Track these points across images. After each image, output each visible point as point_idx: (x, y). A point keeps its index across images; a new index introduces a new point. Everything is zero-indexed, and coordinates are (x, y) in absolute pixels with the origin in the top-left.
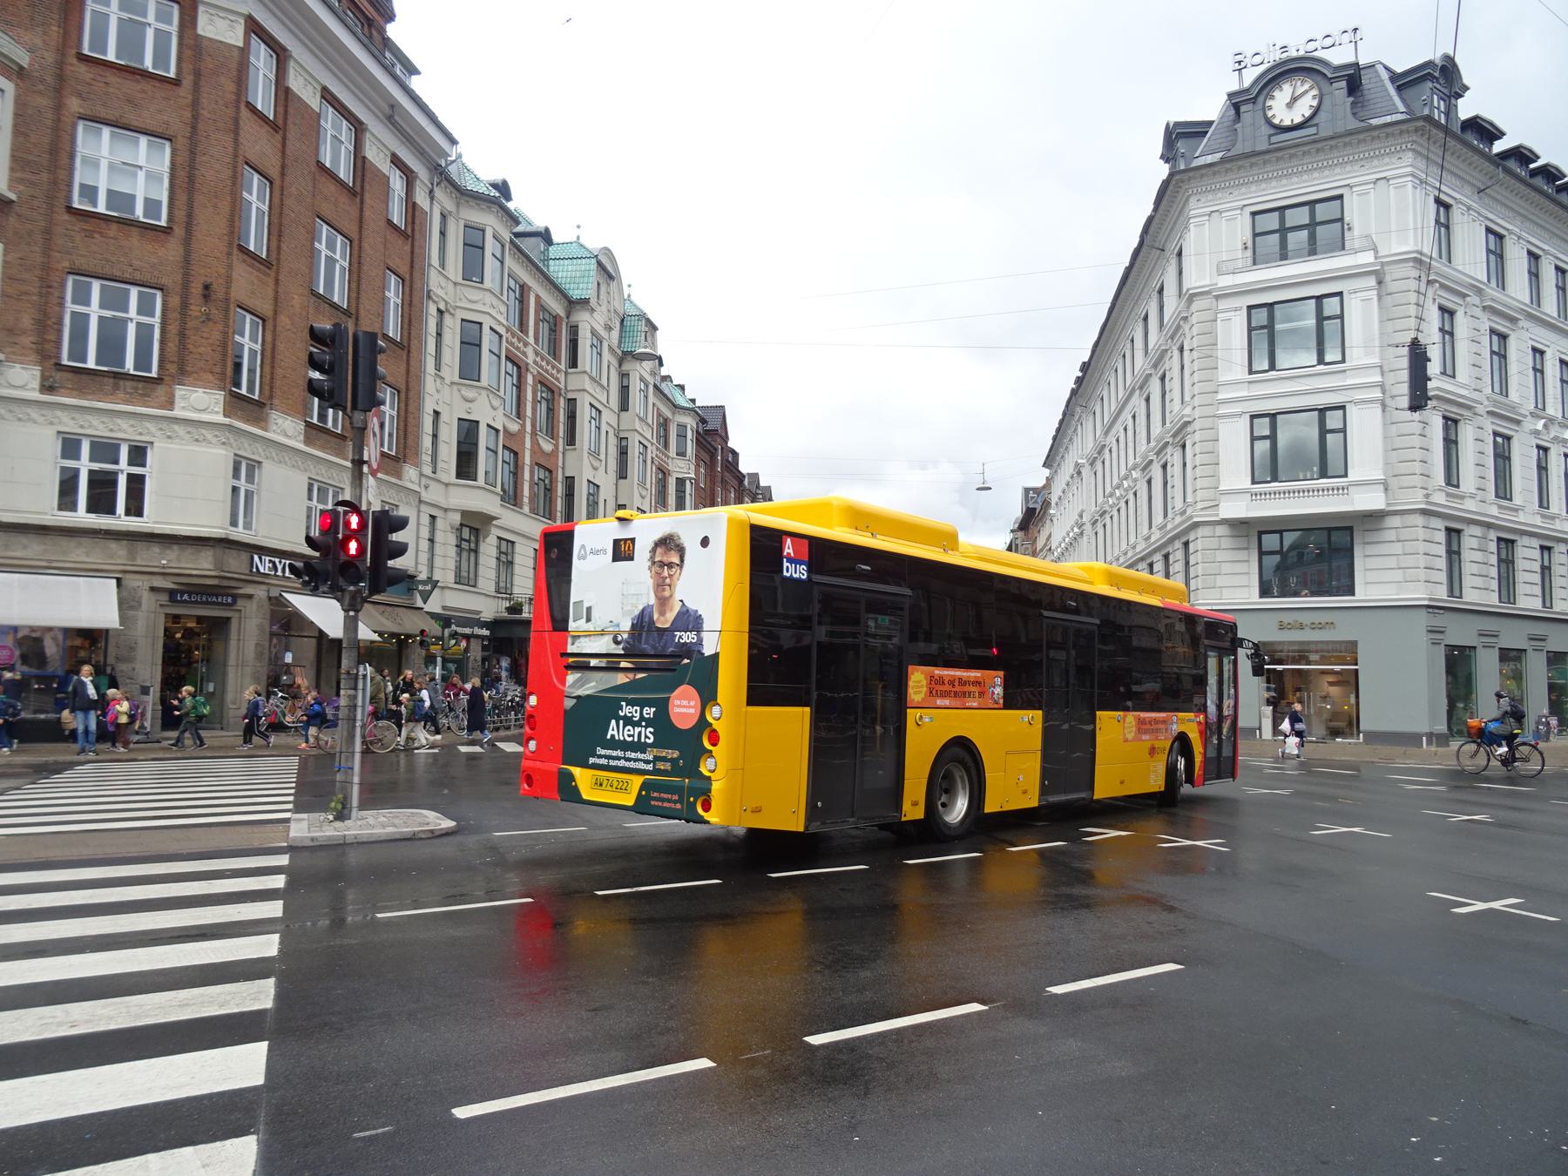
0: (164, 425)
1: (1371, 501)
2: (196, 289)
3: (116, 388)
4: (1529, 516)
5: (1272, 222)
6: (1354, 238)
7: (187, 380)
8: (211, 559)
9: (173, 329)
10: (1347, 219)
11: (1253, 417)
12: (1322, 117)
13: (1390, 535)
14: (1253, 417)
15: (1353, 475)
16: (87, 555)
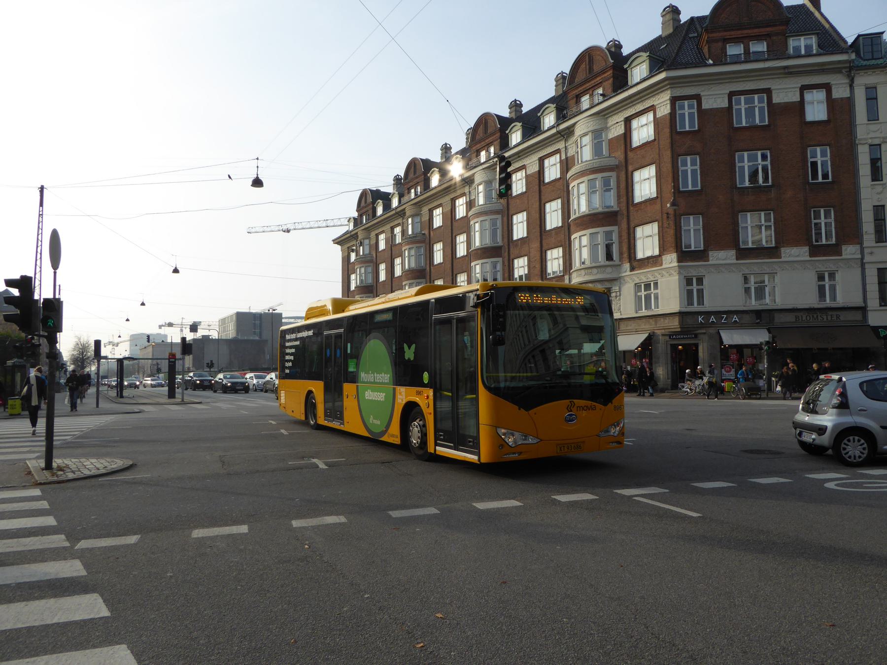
0: (660, 272)
2: (665, 216)
3: (648, 263)
7: (665, 253)
8: (678, 321)
16: (645, 325)
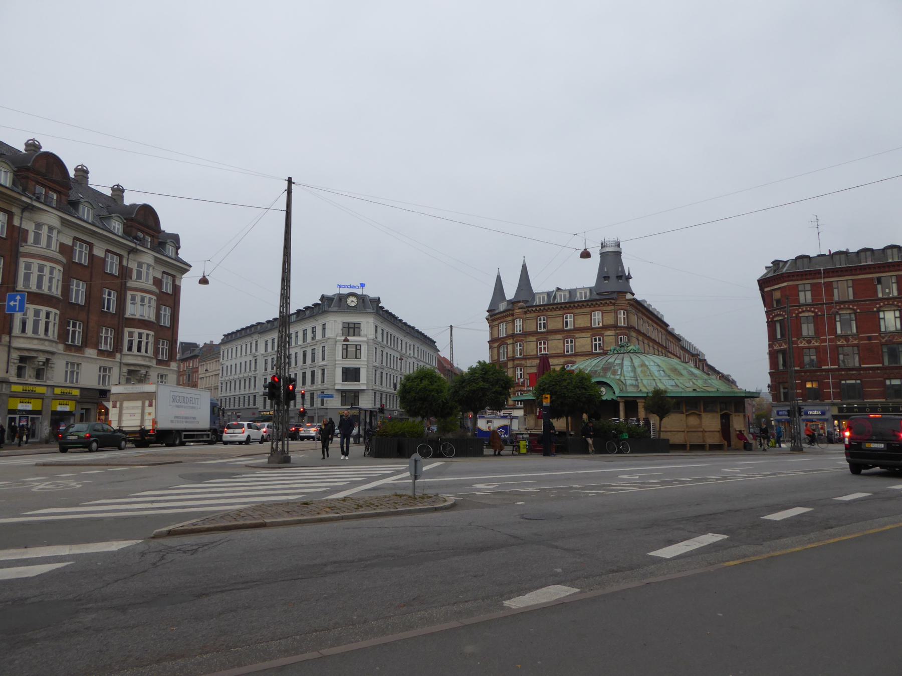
1: (364, 387)
4: (384, 389)
5: (347, 325)
6: (362, 333)
9: (170, 349)
10: (361, 328)
11: (343, 368)
12: (358, 306)
13: (365, 394)
14: (343, 368)
15: (361, 382)
